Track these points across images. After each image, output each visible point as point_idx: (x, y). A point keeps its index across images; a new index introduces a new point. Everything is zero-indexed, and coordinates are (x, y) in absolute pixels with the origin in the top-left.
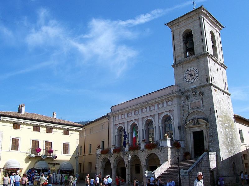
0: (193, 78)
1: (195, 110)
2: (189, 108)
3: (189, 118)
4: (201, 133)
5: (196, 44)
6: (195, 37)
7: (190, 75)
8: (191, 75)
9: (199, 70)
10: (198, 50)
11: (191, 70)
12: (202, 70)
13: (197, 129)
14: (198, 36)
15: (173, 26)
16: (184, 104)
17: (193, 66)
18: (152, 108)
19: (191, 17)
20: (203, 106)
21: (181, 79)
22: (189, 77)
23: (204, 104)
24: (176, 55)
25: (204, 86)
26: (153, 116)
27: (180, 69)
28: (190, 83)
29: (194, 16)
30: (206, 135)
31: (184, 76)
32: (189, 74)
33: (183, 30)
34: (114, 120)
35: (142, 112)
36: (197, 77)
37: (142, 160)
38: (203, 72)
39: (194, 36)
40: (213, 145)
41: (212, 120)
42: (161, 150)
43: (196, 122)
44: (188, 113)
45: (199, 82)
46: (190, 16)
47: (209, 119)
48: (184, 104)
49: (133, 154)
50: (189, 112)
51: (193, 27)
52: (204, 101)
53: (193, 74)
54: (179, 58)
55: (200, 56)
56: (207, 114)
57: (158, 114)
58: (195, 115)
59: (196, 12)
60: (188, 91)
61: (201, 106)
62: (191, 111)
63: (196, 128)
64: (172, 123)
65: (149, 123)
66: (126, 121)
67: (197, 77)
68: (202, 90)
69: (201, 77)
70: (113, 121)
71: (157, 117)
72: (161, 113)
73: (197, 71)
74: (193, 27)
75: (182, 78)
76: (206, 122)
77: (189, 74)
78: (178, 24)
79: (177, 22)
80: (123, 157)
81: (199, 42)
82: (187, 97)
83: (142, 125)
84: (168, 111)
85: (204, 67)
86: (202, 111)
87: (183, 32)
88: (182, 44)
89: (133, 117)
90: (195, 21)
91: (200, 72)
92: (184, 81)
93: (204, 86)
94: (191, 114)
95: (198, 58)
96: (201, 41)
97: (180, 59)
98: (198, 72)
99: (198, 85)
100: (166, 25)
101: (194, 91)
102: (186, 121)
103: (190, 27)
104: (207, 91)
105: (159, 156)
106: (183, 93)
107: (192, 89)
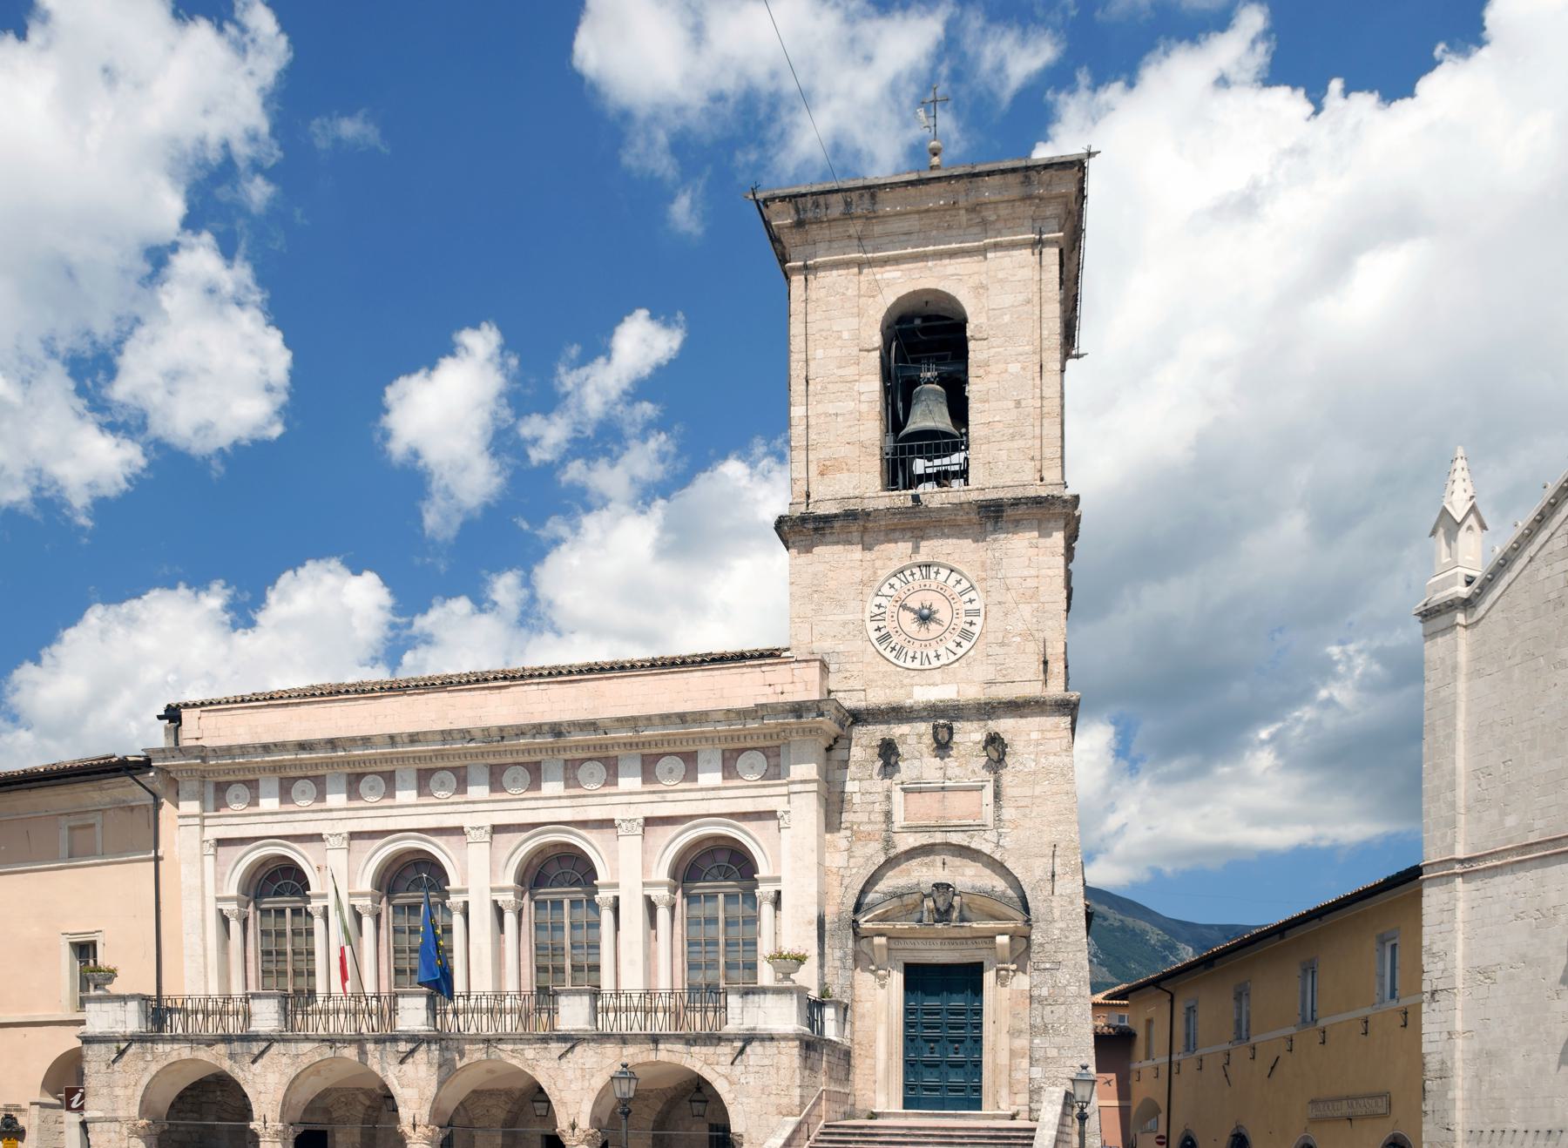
0: (939, 638)
1: (939, 838)
2: (899, 819)
7: (912, 616)
8: (925, 618)
9: (995, 597)
15: (814, 231)
20: (998, 819)
21: (845, 624)
23: (1008, 813)
25: (1017, 707)
28: (909, 664)
29: (1004, 211)
32: (905, 607)
33: (898, 282)
36: (966, 634)
41: (1057, 913)
44: (886, 850)
45: (984, 671)
50: (888, 843)
52: (1008, 791)
53: (944, 614)
54: (845, 476)
59: (1027, 181)
61: (990, 822)
67: (966, 634)
68: (1005, 726)
69: (1002, 644)
75: (850, 617)
77: (905, 607)
78: (855, 228)
81: (1012, 404)
84: (731, 815)
85: (1031, 583)
86: (987, 848)
87: (889, 298)
93: (1017, 707)
95: (994, 515)
101: (943, 721)
107: (934, 712)
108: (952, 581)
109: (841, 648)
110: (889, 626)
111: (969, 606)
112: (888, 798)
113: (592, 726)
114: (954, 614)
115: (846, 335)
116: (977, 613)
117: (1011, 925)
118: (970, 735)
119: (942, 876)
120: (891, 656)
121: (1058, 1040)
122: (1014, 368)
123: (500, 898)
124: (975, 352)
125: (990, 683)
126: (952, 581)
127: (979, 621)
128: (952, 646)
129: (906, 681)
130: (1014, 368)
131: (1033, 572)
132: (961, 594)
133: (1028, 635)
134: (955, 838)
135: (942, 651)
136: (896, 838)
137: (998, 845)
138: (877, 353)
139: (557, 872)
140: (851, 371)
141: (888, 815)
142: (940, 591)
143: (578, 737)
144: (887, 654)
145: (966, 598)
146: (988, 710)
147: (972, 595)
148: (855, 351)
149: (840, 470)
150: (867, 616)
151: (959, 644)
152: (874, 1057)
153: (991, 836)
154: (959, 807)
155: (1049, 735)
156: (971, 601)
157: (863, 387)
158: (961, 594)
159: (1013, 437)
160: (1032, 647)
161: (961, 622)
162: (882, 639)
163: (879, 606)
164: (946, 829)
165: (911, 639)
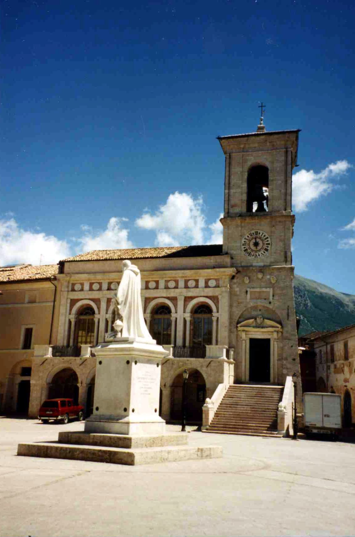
0: (260, 250)
4: (267, 342)
6: (273, 180)
8: (256, 244)
14: (280, 182)
22: (253, 247)
24: (232, 202)
26: (174, 300)
33: (252, 160)
34: (70, 289)
36: (267, 250)
39: (272, 178)
47: (283, 323)
63: (258, 333)
64: (214, 319)
67: (267, 250)
70: (68, 291)
71: (181, 303)
72: (192, 298)
73: (269, 239)
74: (272, 162)
76: (280, 326)
88: (245, 185)
92: (241, 250)
96: (283, 191)
97: (237, 210)
100: (220, 139)
104: (283, 277)
110: (247, 247)
116: (269, 244)
132: (265, 239)
135: (260, 254)
157: (243, 186)
158: (265, 239)
160: (282, 253)
161: (265, 247)
162: (245, 251)
165: (252, 250)
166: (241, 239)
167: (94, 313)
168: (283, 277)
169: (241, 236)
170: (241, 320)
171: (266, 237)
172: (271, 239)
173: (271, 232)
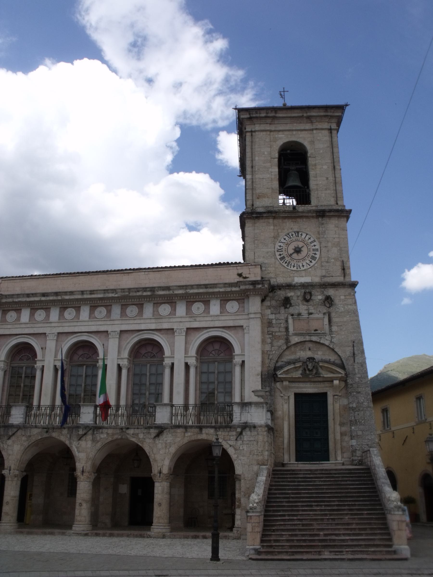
0: (303, 259)
1: (308, 338)
3: (286, 358)
5: (318, 180)
6: (315, 165)
8: (298, 251)
9: (323, 244)
10: (320, 197)
11: (300, 238)
12: (330, 244)
13: (309, 389)
16: (272, 317)
17: (308, 229)
18: (165, 309)
19: (309, 118)
20: (330, 330)
21: (267, 252)
23: (334, 328)
25: (334, 285)
27: (264, 229)
28: (292, 268)
30: (334, 407)
31: (277, 247)
33: (283, 138)
35: (123, 314)
36: (313, 258)
37: (158, 457)
38: (335, 250)
40: (360, 433)
41: (357, 371)
42: (241, 433)
43: (310, 369)
45: (320, 272)
46: (309, 114)
48: (272, 317)
49: (115, 437)
50: (287, 340)
51: (312, 142)
52: (334, 320)
54: (266, 199)
55: (330, 211)
56: (345, 353)
57: (187, 329)
58: (304, 350)
60: (290, 286)
62: (295, 340)
65: (147, 351)
66: (52, 330)
67: (313, 258)
68: (331, 292)
69: (327, 262)
75: (270, 250)
78: (269, 121)
79: (269, 115)
80: (67, 443)
81: (325, 179)
82: (287, 302)
83: (119, 352)
86: (327, 343)
87: (280, 143)
89: (84, 323)
90: (318, 131)
91: (324, 249)
93: (334, 285)
94: (293, 349)
96: (331, 179)
98: (317, 247)
99: (317, 280)
101: (307, 290)
102: (277, 362)
103: (303, 138)
105: (231, 451)
106: (273, 288)
107: (303, 286)
108: (307, 238)
109: (266, 261)
110: (284, 254)
111: (314, 248)
112: (287, 321)
113: (168, 288)
114: (309, 250)
115: (266, 153)
116: (317, 250)
117: (340, 375)
118: (318, 297)
119: (309, 354)
120: (285, 265)
121: (362, 427)
122: (325, 167)
123: (121, 363)
124: (311, 161)
125: (324, 276)
126: (307, 238)
127: (318, 253)
128: (308, 262)
129: (291, 275)
130: (325, 167)
131: (337, 236)
132: (311, 243)
133: (336, 259)
134: (314, 338)
135: (304, 264)
136: (291, 338)
137: (331, 342)
138: (277, 160)
139: (147, 351)
140: (268, 165)
141: (287, 329)
142: (303, 241)
143: (161, 293)
144: (284, 264)
145: (313, 244)
146: (324, 286)
147: (315, 243)
148: (269, 158)
149: (265, 197)
150: (276, 249)
151: (311, 262)
152: (283, 437)
153: (328, 337)
154: (314, 325)
155: (348, 297)
156: (315, 246)
157: (273, 170)
158: (311, 243)
159: (326, 189)
160: (339, 264)
161: (311, 253)
163: (280, 246)
164: (310, 335)
166: (275, 244)
167: (35, 355)
168: (342, 297)
169: (274, 237)
170: (279, 364)
171: (312, 239)
172: (320, 243)
173: (319, 233)
